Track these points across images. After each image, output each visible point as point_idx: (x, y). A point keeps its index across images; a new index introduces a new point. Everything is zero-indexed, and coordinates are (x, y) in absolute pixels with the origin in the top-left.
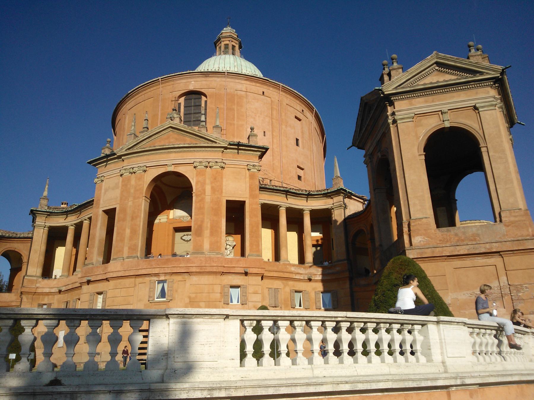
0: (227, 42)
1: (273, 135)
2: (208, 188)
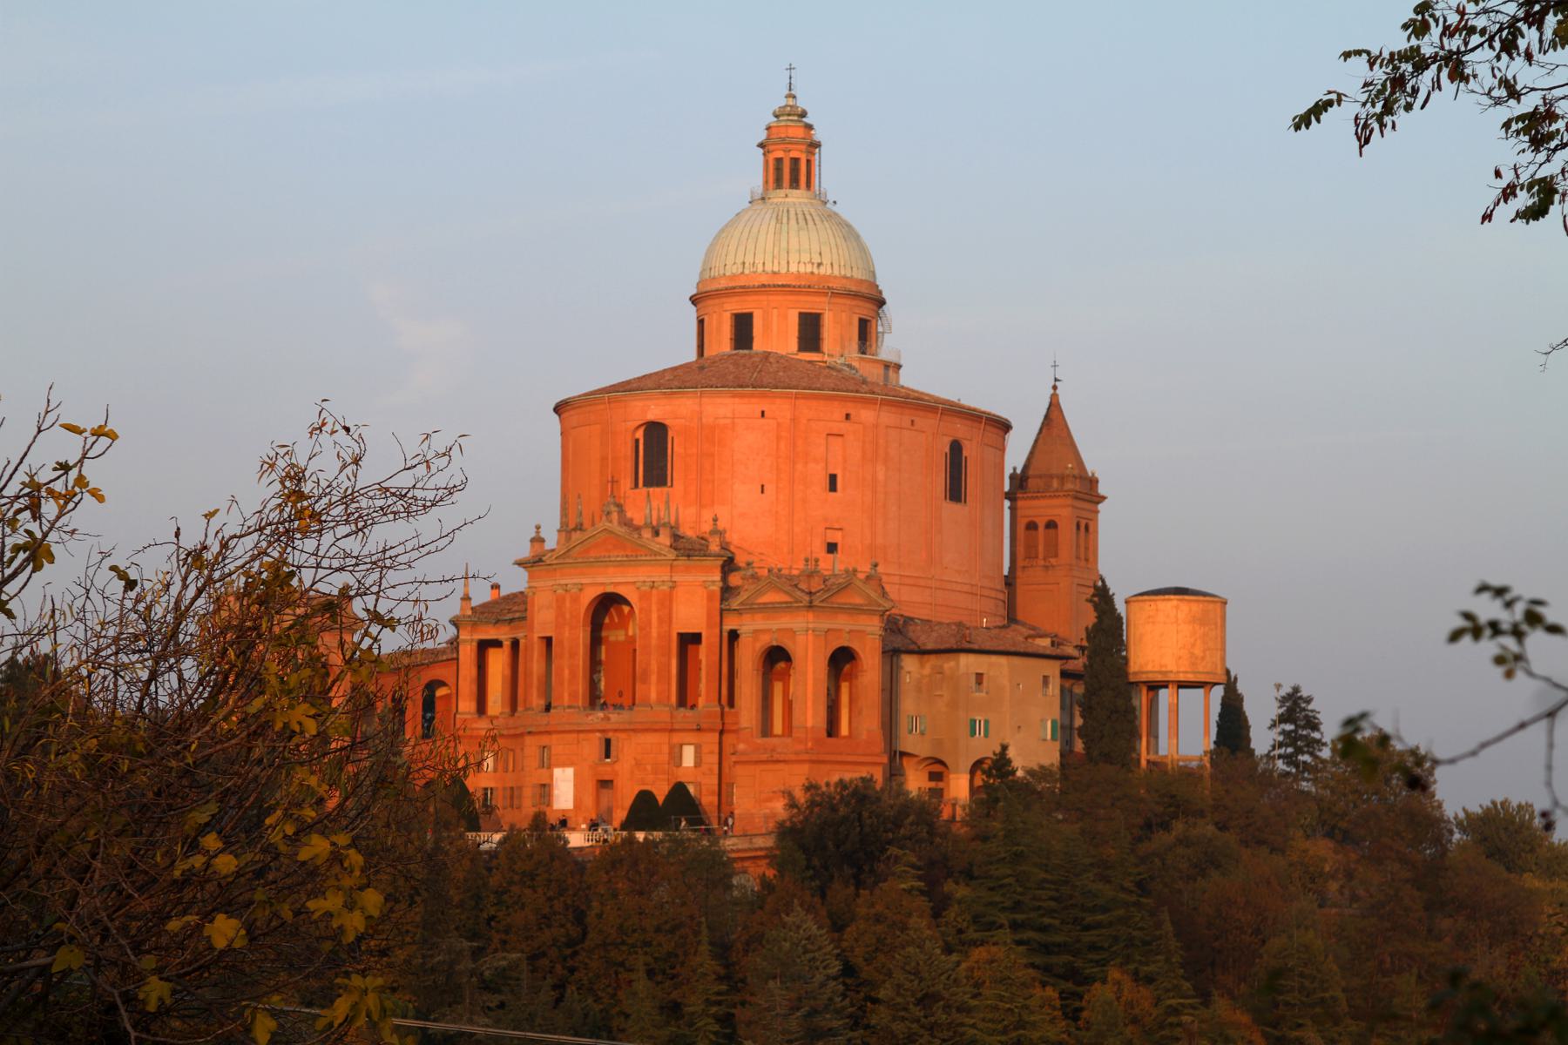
0: (780, 154)
1: (777, 487)
2: (654, 616)
